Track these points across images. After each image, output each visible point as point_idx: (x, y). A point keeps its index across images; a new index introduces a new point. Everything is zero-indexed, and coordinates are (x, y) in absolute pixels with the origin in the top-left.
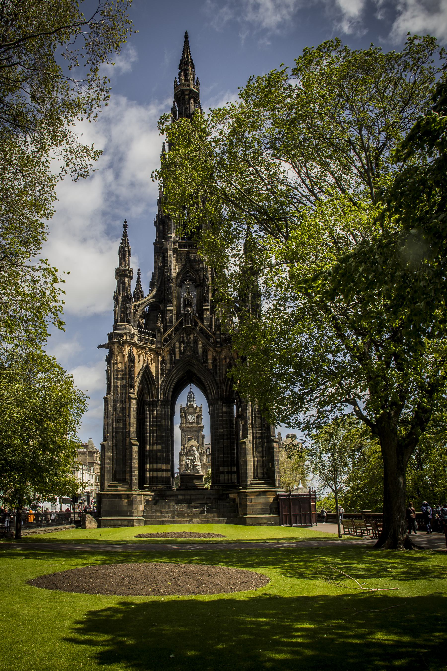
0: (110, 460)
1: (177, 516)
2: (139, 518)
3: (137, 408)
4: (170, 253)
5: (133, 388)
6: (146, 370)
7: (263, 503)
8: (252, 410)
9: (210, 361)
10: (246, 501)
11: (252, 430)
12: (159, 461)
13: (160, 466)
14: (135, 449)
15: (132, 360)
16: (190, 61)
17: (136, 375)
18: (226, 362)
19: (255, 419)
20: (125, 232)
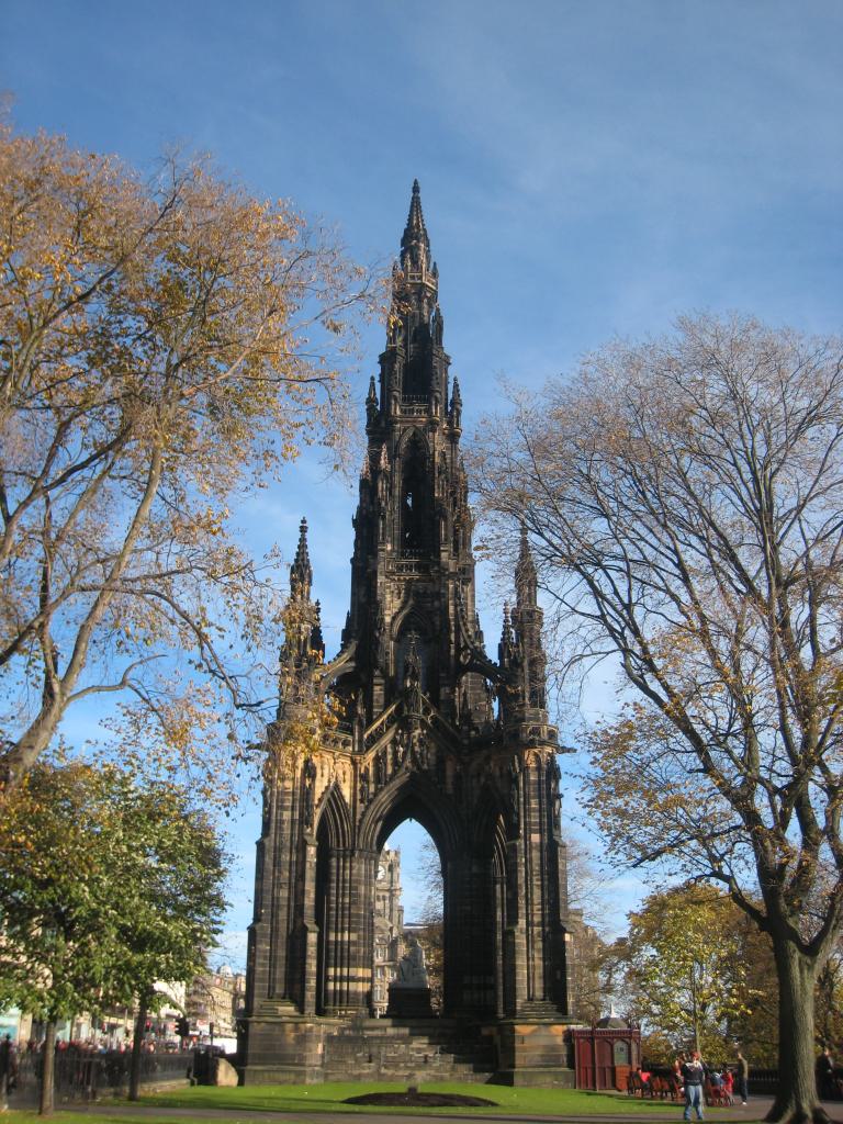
0: (265, 958)
1: (386, 1067)
2: (316, 1068)
3: (318, 864)
4: (381, 579)
5: (312, 826)
6: (334, 792)
7: (545, 1047)
8: (526, 873)
9: (449, 780)
10: (514, 1043)
11: (527, 910)
12: (351, 962)
13: (353, 971)
14: (312, 938)
15: (309, 771)
16: (422, 232)
17: (316, 802)
18: (479, 781)
19: (532, 888)
20: (303, 540)
